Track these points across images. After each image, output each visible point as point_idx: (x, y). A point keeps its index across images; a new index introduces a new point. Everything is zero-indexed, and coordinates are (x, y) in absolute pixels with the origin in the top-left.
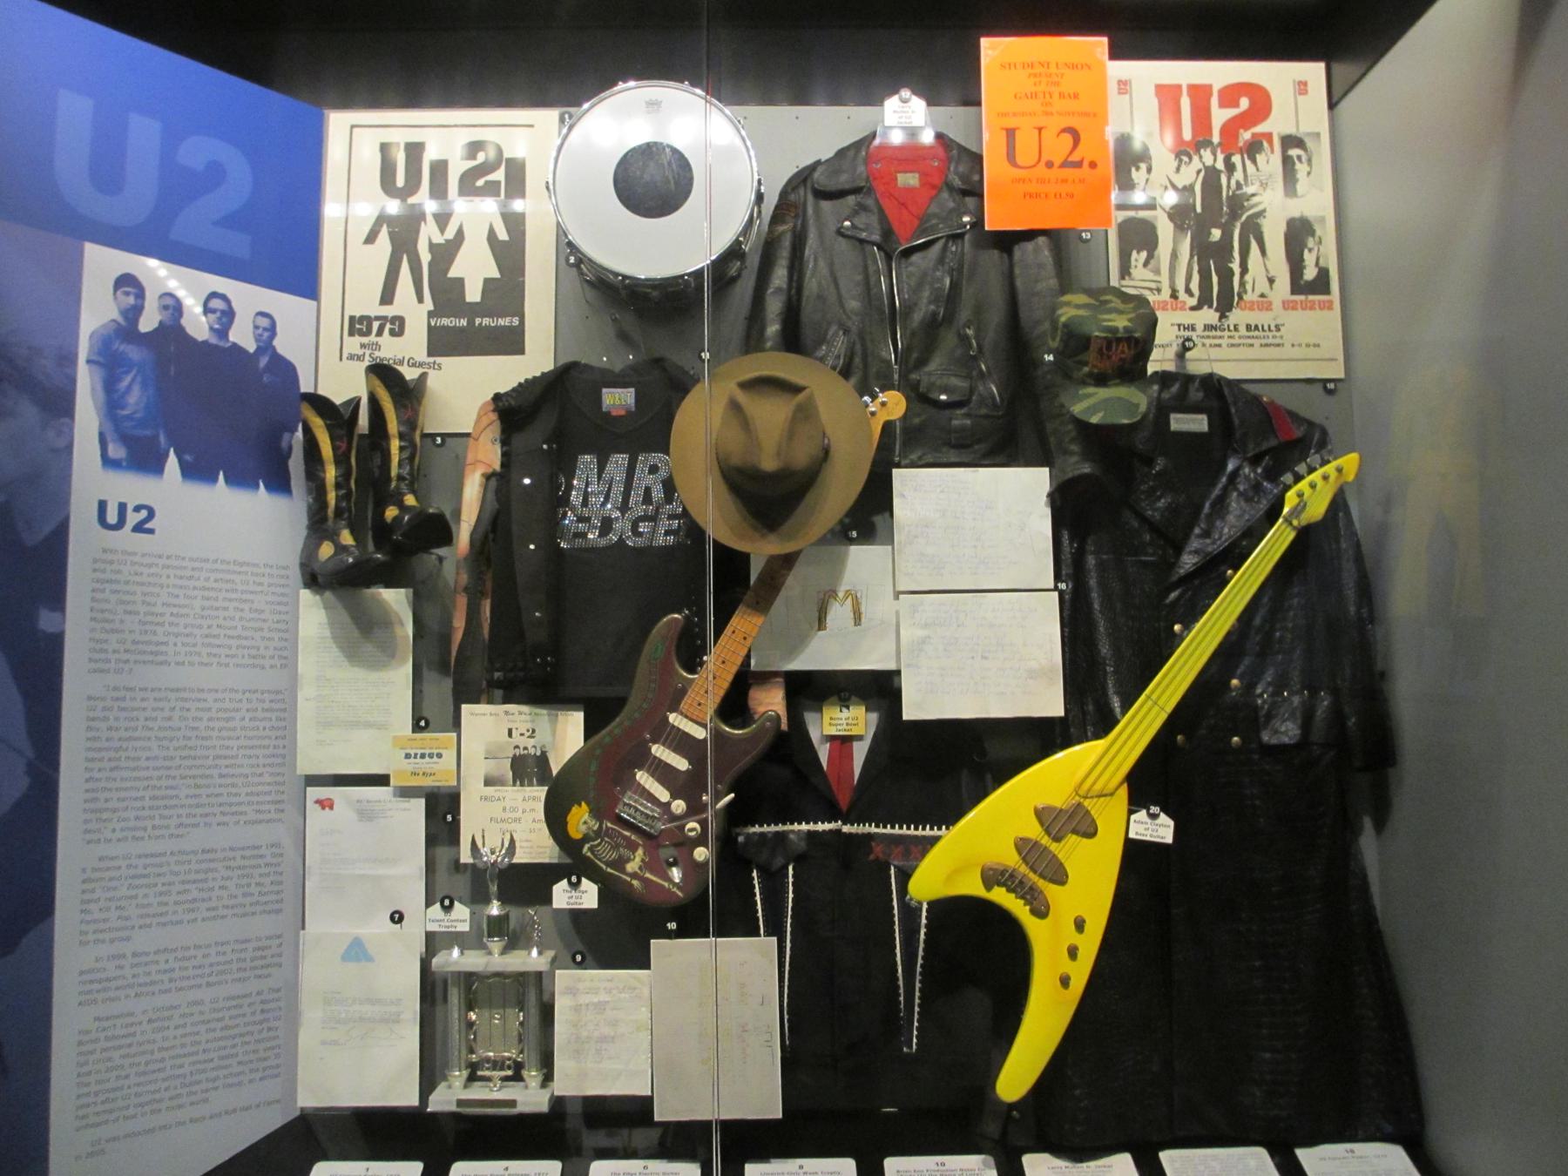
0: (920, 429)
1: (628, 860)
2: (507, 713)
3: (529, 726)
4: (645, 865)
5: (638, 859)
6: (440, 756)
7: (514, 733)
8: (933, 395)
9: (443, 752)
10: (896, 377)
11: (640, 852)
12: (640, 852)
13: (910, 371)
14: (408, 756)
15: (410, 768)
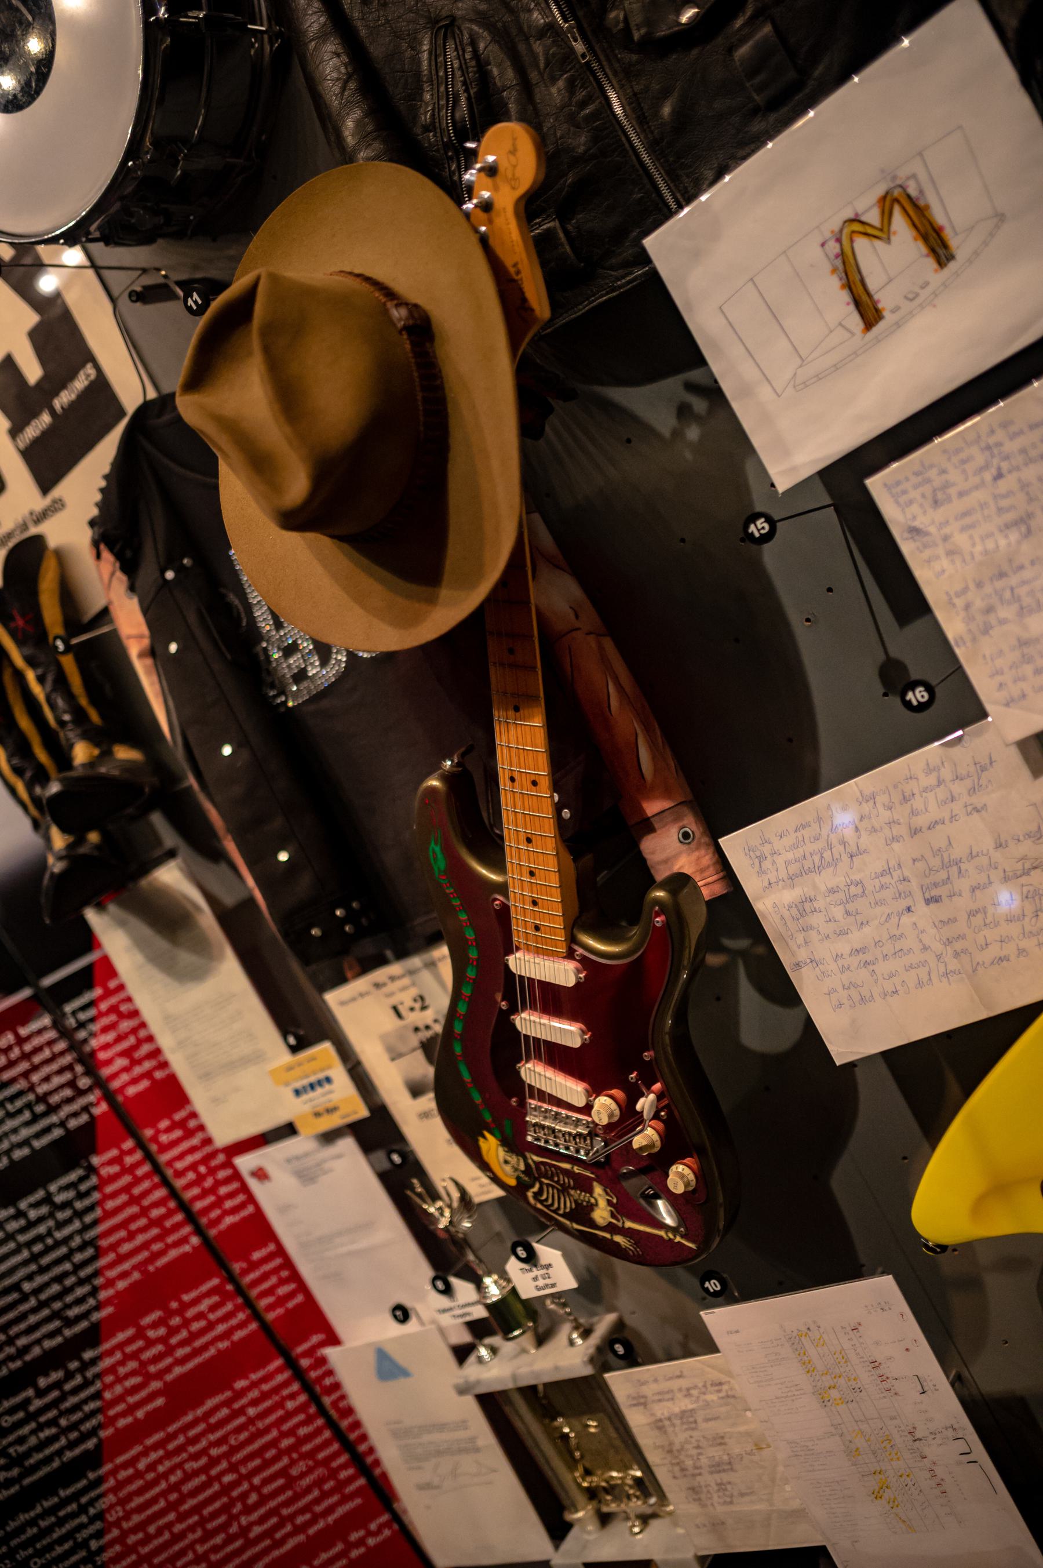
0: (682, 120)
1: (591, 1207)
2: (377, 986)
3: (413, 992)
4: (620, 1209)
5: (602, 1203)
6: (328, 1080)
7: (402, 1010)
8: (662, 32)
9: (330, 1073)
10: (579, 47)
11: (598, 1190)
12: (598, 1190)
13: (604, 11)
14: (297, 1093)
15: (307, 1108)
